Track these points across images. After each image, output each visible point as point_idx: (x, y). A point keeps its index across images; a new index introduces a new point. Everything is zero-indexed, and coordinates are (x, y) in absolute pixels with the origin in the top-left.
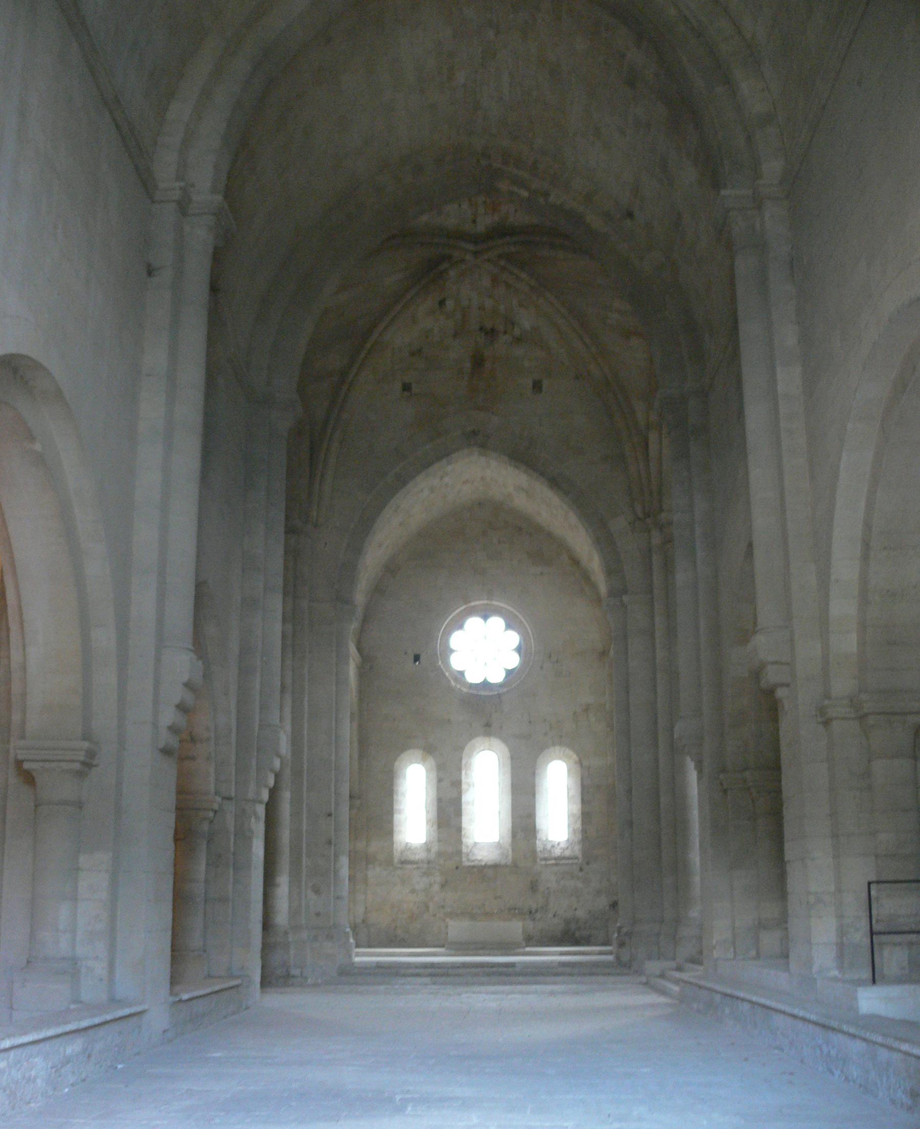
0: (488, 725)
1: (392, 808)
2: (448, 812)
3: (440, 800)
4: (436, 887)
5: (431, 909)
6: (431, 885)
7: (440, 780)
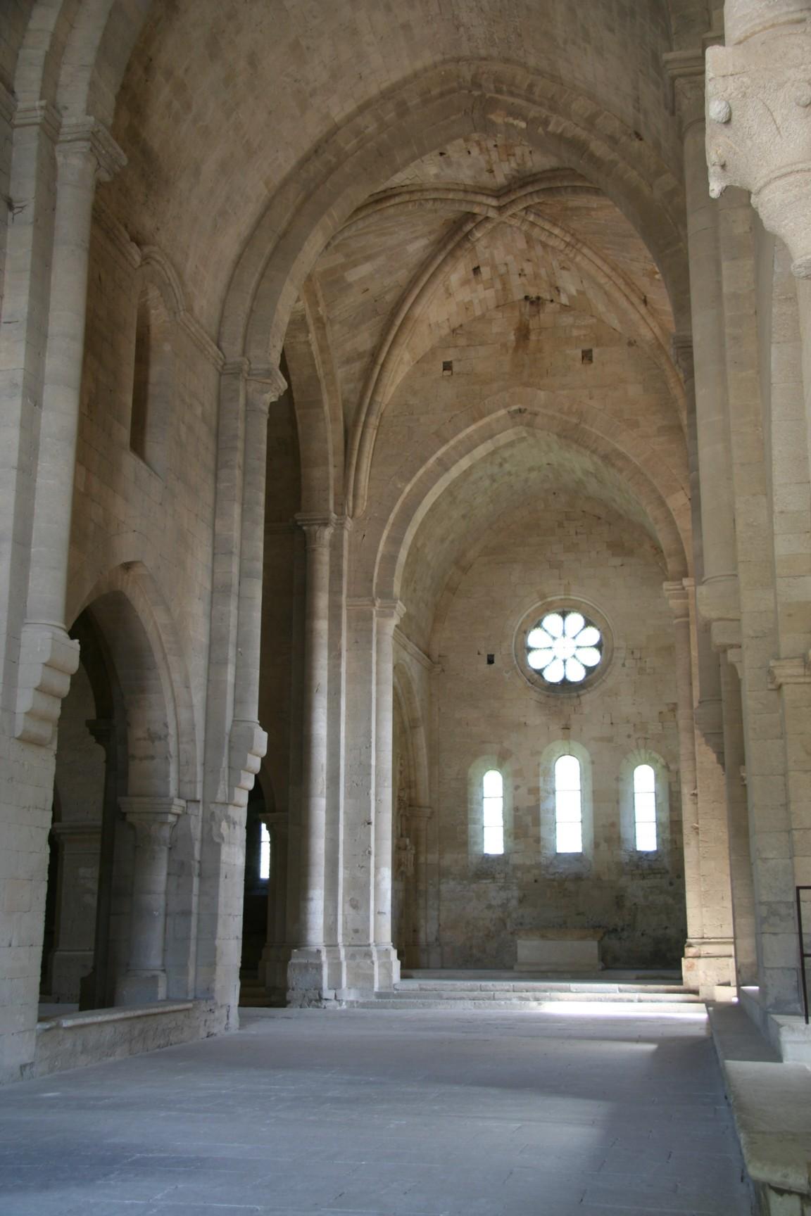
0: (567, 728)
1: (466, 817)
2: (527, 820)
3: (516, 809)
4: (514, 903)
5: (508, 925)
6: (508, 900)
7: (517, 788)
